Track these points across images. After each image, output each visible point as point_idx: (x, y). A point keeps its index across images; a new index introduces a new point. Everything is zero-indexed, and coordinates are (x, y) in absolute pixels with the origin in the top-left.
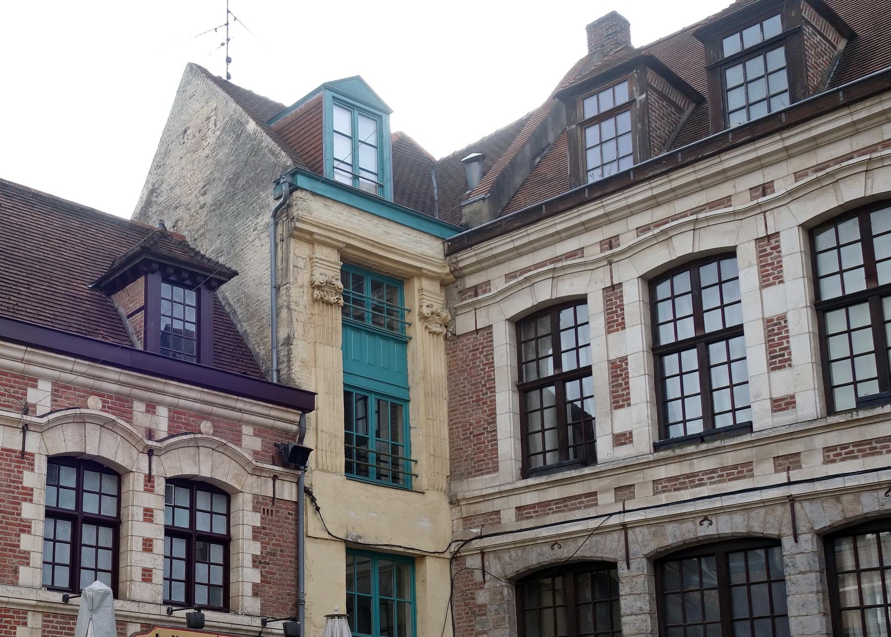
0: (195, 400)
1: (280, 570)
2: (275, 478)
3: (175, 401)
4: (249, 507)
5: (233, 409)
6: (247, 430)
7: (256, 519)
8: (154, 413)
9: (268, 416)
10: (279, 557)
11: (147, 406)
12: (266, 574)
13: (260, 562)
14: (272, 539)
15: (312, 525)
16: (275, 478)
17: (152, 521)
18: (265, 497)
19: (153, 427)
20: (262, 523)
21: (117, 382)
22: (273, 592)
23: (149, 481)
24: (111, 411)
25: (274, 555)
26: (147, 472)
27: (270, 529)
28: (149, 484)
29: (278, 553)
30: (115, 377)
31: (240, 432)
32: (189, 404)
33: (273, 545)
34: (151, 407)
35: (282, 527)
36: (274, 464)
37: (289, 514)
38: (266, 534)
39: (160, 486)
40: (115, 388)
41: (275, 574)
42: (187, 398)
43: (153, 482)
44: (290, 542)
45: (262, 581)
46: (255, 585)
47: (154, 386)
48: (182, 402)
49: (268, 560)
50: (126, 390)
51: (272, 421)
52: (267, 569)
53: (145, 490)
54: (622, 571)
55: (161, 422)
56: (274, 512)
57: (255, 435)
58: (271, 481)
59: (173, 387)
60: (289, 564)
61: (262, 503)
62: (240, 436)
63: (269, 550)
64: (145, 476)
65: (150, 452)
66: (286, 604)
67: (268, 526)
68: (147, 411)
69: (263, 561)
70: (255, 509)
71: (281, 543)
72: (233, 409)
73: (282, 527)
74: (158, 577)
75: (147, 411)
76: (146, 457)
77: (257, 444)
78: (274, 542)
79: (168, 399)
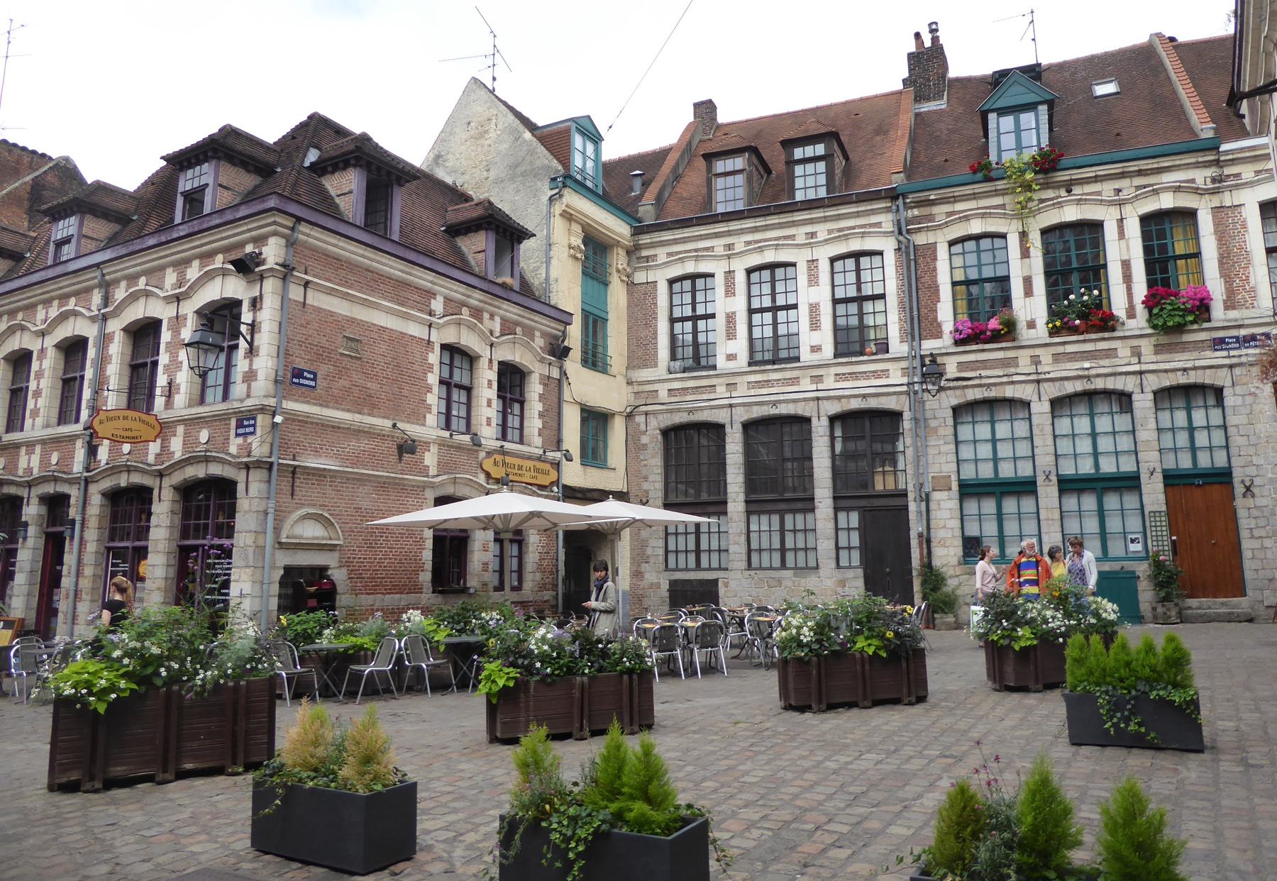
2: (550, 364)
5: (533, 320)
6: (537, 334)
9: (548, 326)
15: (567, 396)
16: (550, 364)
34: (492, 316)
39: (496, 367)
40: (476, 303)
46: (539, 429)
50: (482, 305)
54: (728, 429)
59: (505, 305)
72: (533, 320)
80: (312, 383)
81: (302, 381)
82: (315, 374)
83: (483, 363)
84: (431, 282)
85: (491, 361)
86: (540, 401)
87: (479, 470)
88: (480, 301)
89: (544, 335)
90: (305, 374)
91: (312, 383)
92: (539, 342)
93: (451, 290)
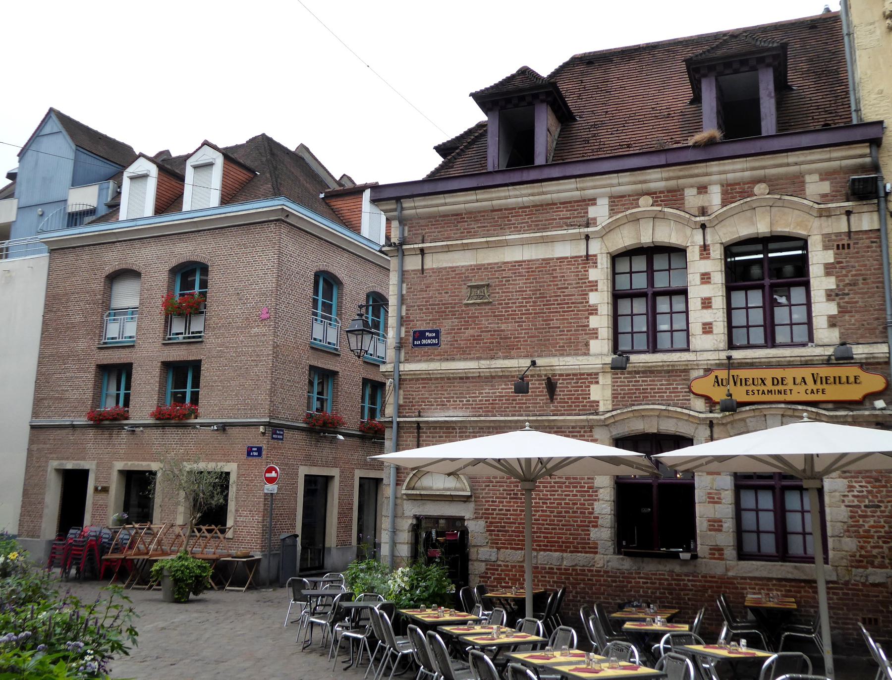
0: (743, 170)
1: (862, 298)
2: (848, 213)
3: (723, 176)
4: (820, 247)
5: (788, 165)
7: (829, 257)
8: (706, 192)
9: (830, 160)
10: (861, 286)
11: (698, 188)
12: (845, 304)
13: (837, 295)
14: (851, 271)
16: (848, 213)
17: (709, 283)
18: (838, 234)
19: (706, 204)
20: (835, 258)
21: (662, 180)
22: (856, 320)
23: (705, 250)
24: (663, 203)
25: (855, 284)
26: (702, 243)
27: (847, 262)
28: (705, 253)
29: (861, 282)
30: (658, 176)
31: (803, 182)
32: (739, 175)
33: (852, 276)
34: (702, 189)
35: (863, 256)
36: (848, 200)
37: (873, 242)
38: (842, 268)
39: (717, 252)
41: (857, 302)
42: (734, 171)
43: (709, 250)
44: (875, 269)
45: (839, 312)
47: (696, 171)
48: (730, 176)
49: (846, 291)
50: (672, 183)
51: (838, 163)
52: (846, 300)
53: (701, 258)
55: (715, 197)
56: (852, 246)
57: (822, 180)
58: (844, 218)
59: (714, 167)
60: (876, 289)
61: (834, 241)
62: (804, 186)
63: (847, 282)
64: (701, 247)
65: (703, 227)
66: (875, 329)
67: (844, 260)
68: (699, 193)
69: (840, 293)
70: (826, 248)
71: (863, 272)
72: (788, 165)
73: (863, 256)
74: (720, 327)
75: (699, 193)
76: (701, 231)
77: (826, 187)
78: (854, 273)
79: (715, 178)
80: (435, 341)
81: (424, 342)
82: (437, 332)
83: (693, 254)
84: (577, 189)
85: (705, 248)
86: (828, 274)
87: (692, 396)
88: (667, 179)
89: (825, 175)
90: (427, 334)
91: (435, 341)
92: (816, 187)
93: (612, 186)
